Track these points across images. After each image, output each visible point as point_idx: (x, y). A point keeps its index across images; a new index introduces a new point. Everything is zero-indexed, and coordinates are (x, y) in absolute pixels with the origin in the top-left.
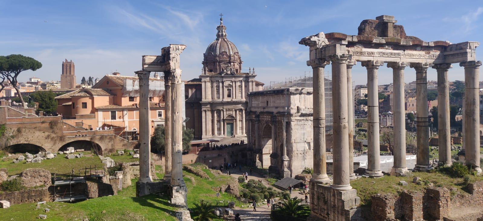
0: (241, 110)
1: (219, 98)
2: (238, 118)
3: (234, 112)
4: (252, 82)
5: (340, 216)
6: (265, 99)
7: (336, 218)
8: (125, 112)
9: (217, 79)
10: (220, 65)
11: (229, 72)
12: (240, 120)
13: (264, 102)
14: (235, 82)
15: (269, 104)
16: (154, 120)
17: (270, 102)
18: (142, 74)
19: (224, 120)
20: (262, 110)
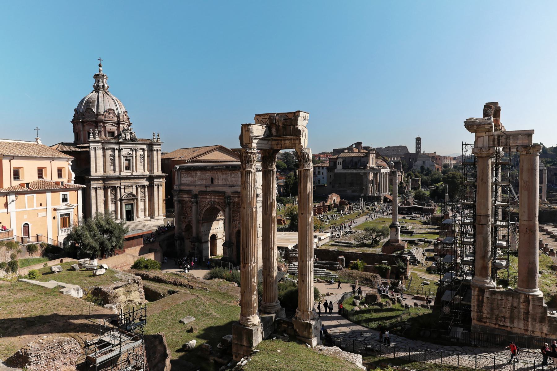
0: (144, 186)
1: (115, 171)
2: (140, 197)
3: (135, 190)
4: (157, 151)
5: (538, 325)
6: (209, 175)
7: (530, 326)
8: (11, 197)
9: (112, 146)
10: (104, 127)
11: (128, 137)
12: (141, 200)
13: (206, 179)
14: (136, 150)
15: (216, 182)
16: (57, 207)
17: (218, 179)
18: (251, 153)
19: (121, 200)
20: (204, 189)
